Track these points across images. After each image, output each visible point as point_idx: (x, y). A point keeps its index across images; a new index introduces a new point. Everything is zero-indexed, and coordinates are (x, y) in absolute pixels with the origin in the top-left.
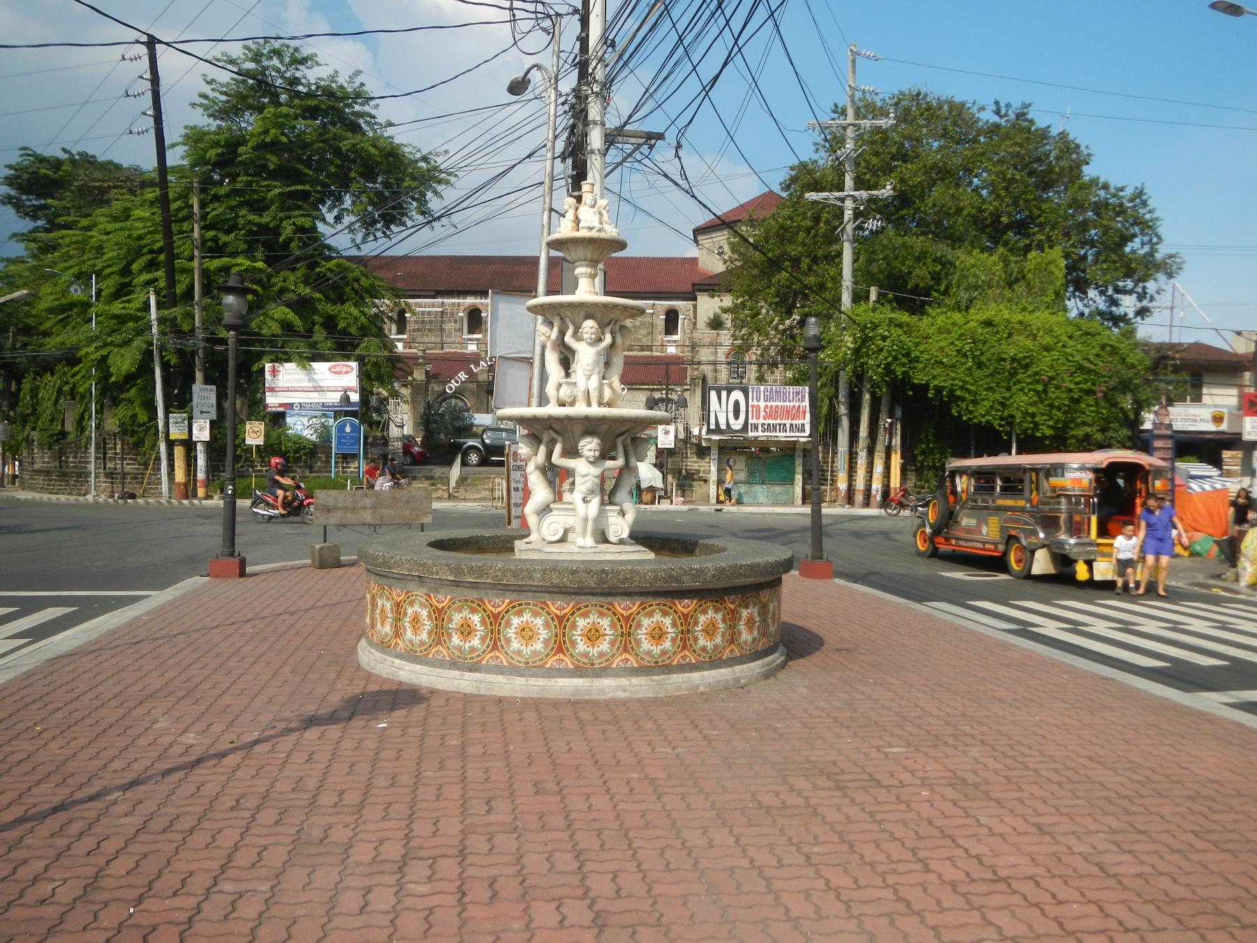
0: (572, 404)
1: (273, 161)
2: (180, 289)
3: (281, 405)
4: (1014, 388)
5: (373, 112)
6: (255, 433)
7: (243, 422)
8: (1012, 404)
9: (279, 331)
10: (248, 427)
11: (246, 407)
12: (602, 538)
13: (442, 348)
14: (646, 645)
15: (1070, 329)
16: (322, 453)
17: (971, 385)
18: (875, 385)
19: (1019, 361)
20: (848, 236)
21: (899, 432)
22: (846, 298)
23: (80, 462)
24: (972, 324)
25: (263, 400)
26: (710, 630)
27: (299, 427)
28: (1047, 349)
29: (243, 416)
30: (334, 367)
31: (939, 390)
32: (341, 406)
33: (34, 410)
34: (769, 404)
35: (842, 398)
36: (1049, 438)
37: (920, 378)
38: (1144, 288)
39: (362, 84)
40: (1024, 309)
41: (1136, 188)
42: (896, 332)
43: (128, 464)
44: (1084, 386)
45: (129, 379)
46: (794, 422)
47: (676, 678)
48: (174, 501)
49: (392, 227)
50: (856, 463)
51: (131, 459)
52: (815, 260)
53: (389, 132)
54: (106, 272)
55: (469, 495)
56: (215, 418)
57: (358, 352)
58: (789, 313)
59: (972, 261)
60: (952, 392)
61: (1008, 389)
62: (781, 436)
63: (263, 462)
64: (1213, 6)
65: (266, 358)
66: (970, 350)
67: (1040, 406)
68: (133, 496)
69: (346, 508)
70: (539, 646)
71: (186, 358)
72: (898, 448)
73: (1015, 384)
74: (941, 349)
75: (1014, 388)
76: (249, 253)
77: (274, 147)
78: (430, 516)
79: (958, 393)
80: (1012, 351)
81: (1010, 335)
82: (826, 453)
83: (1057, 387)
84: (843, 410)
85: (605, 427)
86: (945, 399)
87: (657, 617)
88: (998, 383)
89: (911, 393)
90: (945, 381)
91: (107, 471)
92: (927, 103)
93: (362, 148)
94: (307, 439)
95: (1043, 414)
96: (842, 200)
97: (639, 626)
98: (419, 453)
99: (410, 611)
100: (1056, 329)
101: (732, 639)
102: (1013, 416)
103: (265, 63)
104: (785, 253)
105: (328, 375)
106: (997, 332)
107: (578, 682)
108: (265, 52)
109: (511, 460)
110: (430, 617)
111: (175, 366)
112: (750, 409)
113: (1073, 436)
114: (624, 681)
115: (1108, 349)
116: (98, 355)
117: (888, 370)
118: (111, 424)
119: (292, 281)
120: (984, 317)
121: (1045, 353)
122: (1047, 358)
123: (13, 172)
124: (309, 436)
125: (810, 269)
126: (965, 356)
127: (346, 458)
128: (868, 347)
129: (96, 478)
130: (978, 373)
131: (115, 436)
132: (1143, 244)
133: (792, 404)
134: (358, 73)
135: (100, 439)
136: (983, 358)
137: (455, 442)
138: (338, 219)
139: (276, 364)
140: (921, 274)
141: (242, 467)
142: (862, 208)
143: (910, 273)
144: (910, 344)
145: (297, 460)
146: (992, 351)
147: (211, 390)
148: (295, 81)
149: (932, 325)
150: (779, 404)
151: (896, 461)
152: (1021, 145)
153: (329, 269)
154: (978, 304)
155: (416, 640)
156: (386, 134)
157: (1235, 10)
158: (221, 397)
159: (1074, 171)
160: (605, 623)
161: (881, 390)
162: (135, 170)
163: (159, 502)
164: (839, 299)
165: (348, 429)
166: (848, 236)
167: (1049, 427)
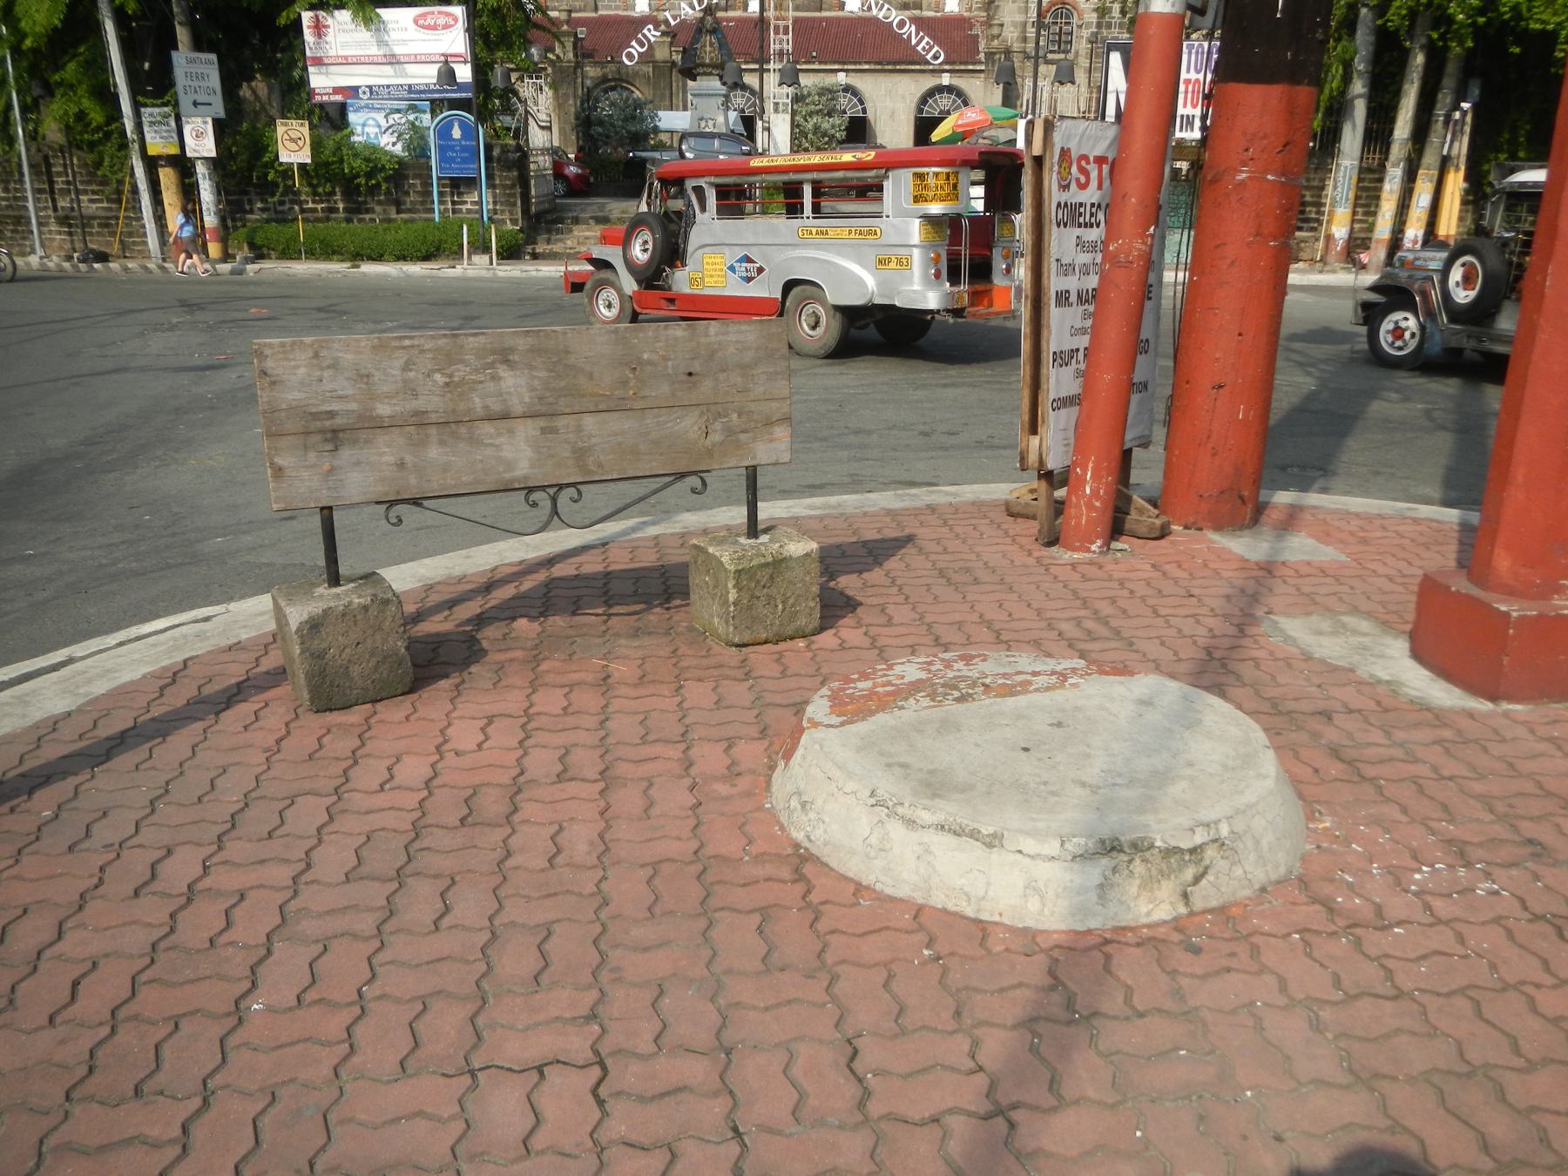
3: (337, 90)
7: (272, 123)
10: (280, 130)
13: (596, 9)
16: (416, 177)
21: (1467, 129)
23: (16, 198)
25: (304, 81)
27: (372, 130)
29: (273, 112)
30: (424, 15)
43: (91, 201)
51: (94, 192)
56: (222, 114)
63: (315, 194)
68: (103, 257)
69: (421, 420)
72: (1463, 159)
78: (782, 432)
84: (1358, 87)
89: (1517, 50)
91: (60, 212)
94: (386, 153)
98: (578, 176)
105: (413, 32)
109: (1051, 180)
112: (1182, 88)
118: (52, 131)
124: (389, 148)
127: (458, 185)
129: (40, 224)
131: (62, 152)
135: (39, 158)
137: (634, 156)
139: (322, 14)
141: (282, 203)
145: (373, 190)
147: (210, 62)
151: (1456, 183)
163: (146, 268)
165: (456, 133)
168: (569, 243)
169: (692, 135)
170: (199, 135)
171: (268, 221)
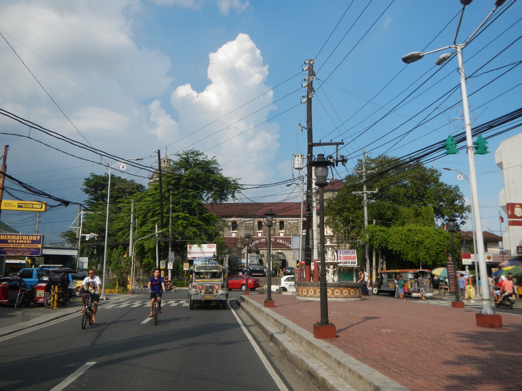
0: (327, 260)
1: (191, 184)
2: (164, 222)
3: (192, 258)
4: (419, 250)
5: (218, 167)
6: (186, 266)
10: (184, 265)
11: (181, 258)
12: (333, 281)
14: (344, 294)
15: (434, 232)
17: (406, 249)
18: (376, 250)
19: (419, 242)
22: (366, 223)
24: (405, 231)
26: (353, 292)
28: (428, 238)
31: (396, 251)
33: (109, 260)
34: (344, 255)
35: (367, 253)
36: (431, 265)
38: (462, 215)
39: (216, 160)
40: (420, 225)
41: (456, 185)
42: (382, 233)
45: (150, 249)
46: (352, 261)
50: (372, 274)
52: (355, 208)
53: (221, 172)
54: (139, 217)
57: (214, 240)
58: (347, 225)
62: (348, 265)
66: (405, 239)
67: (427, 255)
69: (265, 281)
71: (166, 243)
73: (419, 249)
74: (396, 238)
75: (419, 250)
76: (183, 211)
77: (192, 180)
79: (402, 252)
80: (417, 239)
81: (416, 234)
83: (432, 250)
84: (367, 257)
87: (345, 290)
88: (414, 249)
90: (398, 248)
92: (388, 159)
93: (217, 179)
95: (428, 258)
99: (310, 290)
100: (430, 232)
101: (356, 294)
102: (419, 258)
103: (189, 156)
105: (207, 248)
106: (412, 233)
107: (335, 299)
108: (190, 153)
111: (164, 246)
112: (338, 257)
115: (446, 237)
116: (140, 243)
117: (380, 246)
120: (408, 229)
121: (427, 239)
122: (428, 241)
123: (86, 181)
125: (354, 212)
128: (374, 238)
130: (407, 246)
133: (351, 255)
134: (215, 157)
136: (408, 241)
138: (208, 199)
140: (389, 213)
142: (369, 196)
143: (385, 213)
149: (393, 231)
150: (347, 255)
153: (206, 216)
154: (406, 224)
155: (311, 294)
156: (220, 173)
157: (449, 170)
159: (436, 180)
161: (378, 251)
162: (132, 181)
164: (363, 222)
167: (430, 262)
169: (251, 264)
171: (177, 280)
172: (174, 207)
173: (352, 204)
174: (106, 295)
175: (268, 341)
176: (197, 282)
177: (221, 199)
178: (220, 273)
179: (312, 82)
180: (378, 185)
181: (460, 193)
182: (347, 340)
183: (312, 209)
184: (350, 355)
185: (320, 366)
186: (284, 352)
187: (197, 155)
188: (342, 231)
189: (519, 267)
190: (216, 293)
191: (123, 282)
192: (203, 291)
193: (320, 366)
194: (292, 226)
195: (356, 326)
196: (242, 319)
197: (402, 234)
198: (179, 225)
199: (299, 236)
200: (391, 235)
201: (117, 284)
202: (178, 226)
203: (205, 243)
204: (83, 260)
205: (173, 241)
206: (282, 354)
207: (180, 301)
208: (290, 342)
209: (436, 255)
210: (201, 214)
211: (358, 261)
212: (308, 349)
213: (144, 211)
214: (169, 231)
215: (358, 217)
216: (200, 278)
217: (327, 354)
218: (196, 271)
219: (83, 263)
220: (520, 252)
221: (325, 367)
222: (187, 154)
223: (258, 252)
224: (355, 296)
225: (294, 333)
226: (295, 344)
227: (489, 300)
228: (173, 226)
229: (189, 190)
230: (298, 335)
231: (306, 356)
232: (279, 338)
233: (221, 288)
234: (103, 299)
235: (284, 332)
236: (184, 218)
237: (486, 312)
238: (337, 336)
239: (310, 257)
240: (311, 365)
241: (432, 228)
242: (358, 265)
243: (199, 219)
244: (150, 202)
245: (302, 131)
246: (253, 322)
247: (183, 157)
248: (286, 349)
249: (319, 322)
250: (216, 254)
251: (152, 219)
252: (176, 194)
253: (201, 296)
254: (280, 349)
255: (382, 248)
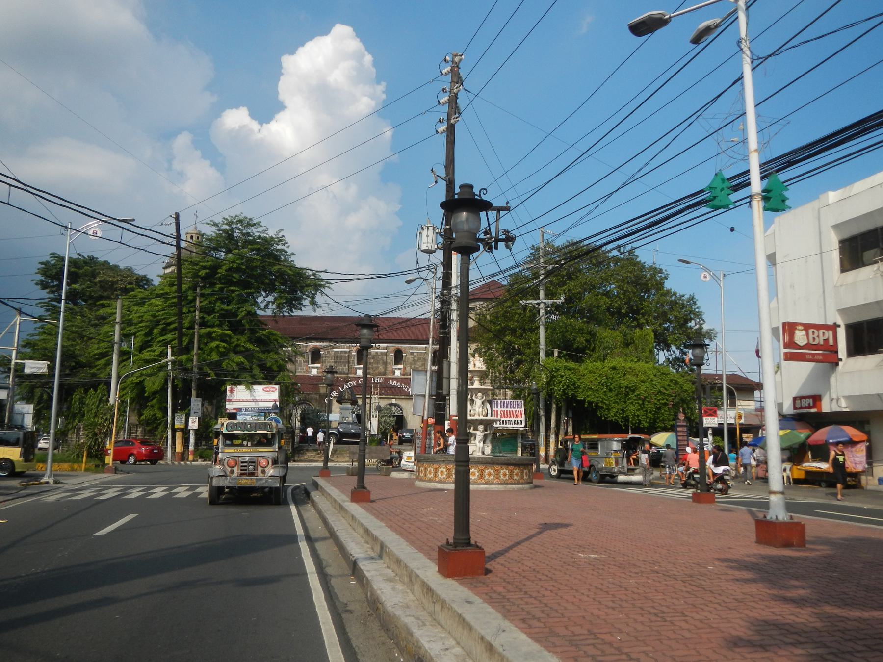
0: (474, 416)
2: (185, 344)
4: (628, 402)
5: (286, 249)
8: (627, 410)
9: (236, 368)
11: (214, 410)
12: (483, 453)
14: (502, 477)
15: (655, 371)
17: (606, 400)
19: (630, 388)
20: (542, 322)
22: (542, 354)
24: (606, 369)
26: (517, 474)
28: (643, 382)
30: (266, 388)
31: (590, 403)
32: (272, 410)
33: (80, 410)
34: (503, 410)
35: (541, 407)
36: (647, 428)
37: (580, 397)
39: (283, 236)
40: (632, 361)
41: (690, 295)
42: (568, 373)
44: (663, 401)
45: (155, 393)
46: (516, 419)
47: (509, 486)
48: (176, 463)
49: (294, 310)
52: (524, 330)
53: (292, 258)
54: (138, 334)
55: (339, 459)
57: (277, 379)
59: (606, 334)
60: (597, 403)
61: (625, 402)
62: (509, 426)
64: (680, 261)
65: (228, 383)
66: (605, 382)
67: (641, 411)
70: (476, 477)
71: (187, 384)
72: (571, 433)
73: (628, 400)
74: (591, 382)
76: (220, 326)
77: (238, 270)
79: (600, 404)
80: (626, 383)
81: (625, 374)
82: (533, 435)
84: (542, 413)
85: (484, 422)
86: (594, 407)
87: (505, 470)
88: (620, 399)
93: (284, 271)
95: (643, 416)
96: (539, 304)
97: (500, 472)
99: (440, 470)
100: (648, 372)
101: (522, 478)
102: (627, 416)
103: (234, 226)
104: (508, 326)
105: (262, 392)
106: (619, 373)
107: (486, 486)
108: (235, 221)
110: (446, 471)
113: (659, 426)
114: (497, 486)
115: (674, 381)
116: (137, 381)
119: (242, 341)
121: (642, 384)
122: (643, 387)
123: (43, 266)
125: (522, 335)
126: (603, 385)
130: (610, 394)
132: (696, 324)
133: (515, 410)
136: (612, 387)
138: (267, 306)
139: (233, 386)
140: (581, 340)
142: (549, 309)
143: (575, 340)
144: (575, 379)
146: (616, 383)
147: (200, 401)
148: (248, 234)
149: (587, 369)
150: (509, 410)
152: (631, 273)
154: (608, 358)
155: (442, 477)
158: (203, 405)
159: (659, 285)
160: (492, 471)
162: (129, 270)
164: (539, 353)
166: (542, 322)
167: (646, 422)
168: (305, 457)
169: (342, 423)
170: (194, 422)
171: (207, 449)
172: (205, 318)
173: (519, 322)
174: (55, 475)
175: (347, 575)
176: (225, 453)
177: (292, 306)
178: (273, 435)
179: (456, 95)
180: (564, 291)
181: (698, 308)
182: (508, 582)
183: (450, 324)
184: (516, 626)
185: (447, 649)
186: (374, 604)
187: (250, 225)
188: (501, 368)
189: (795, 432)
190: (262, 475)
191: (97, 450)
192: (235, 469)
193: (447, 649)
194: (416, 359)
195: (526, 544)
196: (307, 525)
197: (601, 374)
198: (212, 350)
199: (424, 373)
200: (584, 375)
201: (85, 454)
202: (211, 352)
203: (260, 384)
204: (23, 408)
205: (199, 379)
206: (370, 607)
207: (198, 487)
208: (390, 580)
209: (655, 412)
210: (253, 331)
211: (526, 420)
212: (424, 601)
213: (148, 324)
214: (192, 361)
215: (528, 345)
216: (232, 445)
217: (464, 620)
218: (225, 431)
219: (24, 414)
220: (798, 406)
221: (458, 650)
222: (230, 223)
223: (354, 402)
224: (521, 481)
225: (398, 561)
226: (399, 586)
227: (782, 493)
228: (200, 351)
229: (232, 288)
230: (406, 566)
231: (418, 619)
232: (368, 571)
233: (273, 465)
234: (47, 483)
235: (380, 556)
236: (222, 338)
237: (776, 516)
238: (488, 572)
239: (444, 410)
240: (427, 646)
241: (652, 366)
242: (526, 426)
243: (250, 341)
244: (160, 307)
245: (436, 182)
246: (327, 532)
247: (222, 228)
248: (378, 598)
249: (451, 541)
250: (278, 403)
251: (162, 338)
252: (208, 294)
253: (232, 479)
254: (367, 597)
255: (567, 398)
